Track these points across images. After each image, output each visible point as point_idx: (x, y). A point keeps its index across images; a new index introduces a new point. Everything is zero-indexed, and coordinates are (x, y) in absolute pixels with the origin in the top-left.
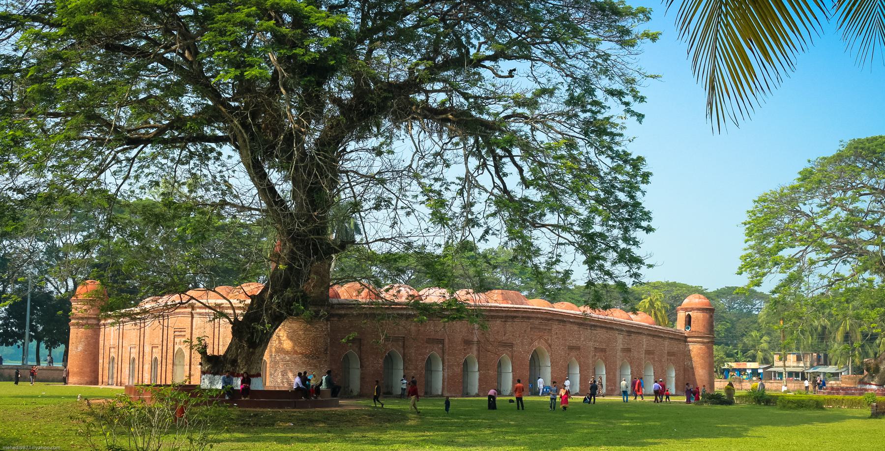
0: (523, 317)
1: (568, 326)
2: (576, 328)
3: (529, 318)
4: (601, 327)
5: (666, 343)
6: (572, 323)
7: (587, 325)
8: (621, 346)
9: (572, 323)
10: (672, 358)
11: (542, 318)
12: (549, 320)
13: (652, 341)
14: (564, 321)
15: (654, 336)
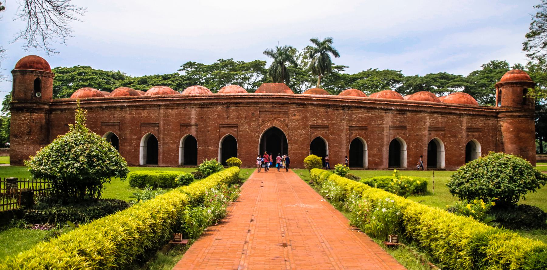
0: (248, 103)
1: (310, 108)
2: (322, 109)
3: (257, 103)
4: (356, 107)
5: (465, 120)
6: (314, 105)
7: (337, 106)
8: (390, 124)
9: (314, 105)
10: (476, 134)
11: (273, 103)
12: (283, 104)
13: (440, 118)
14: (305, 104)
15: (441, 113)
